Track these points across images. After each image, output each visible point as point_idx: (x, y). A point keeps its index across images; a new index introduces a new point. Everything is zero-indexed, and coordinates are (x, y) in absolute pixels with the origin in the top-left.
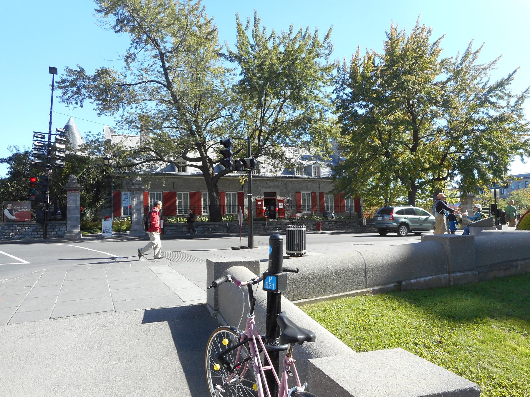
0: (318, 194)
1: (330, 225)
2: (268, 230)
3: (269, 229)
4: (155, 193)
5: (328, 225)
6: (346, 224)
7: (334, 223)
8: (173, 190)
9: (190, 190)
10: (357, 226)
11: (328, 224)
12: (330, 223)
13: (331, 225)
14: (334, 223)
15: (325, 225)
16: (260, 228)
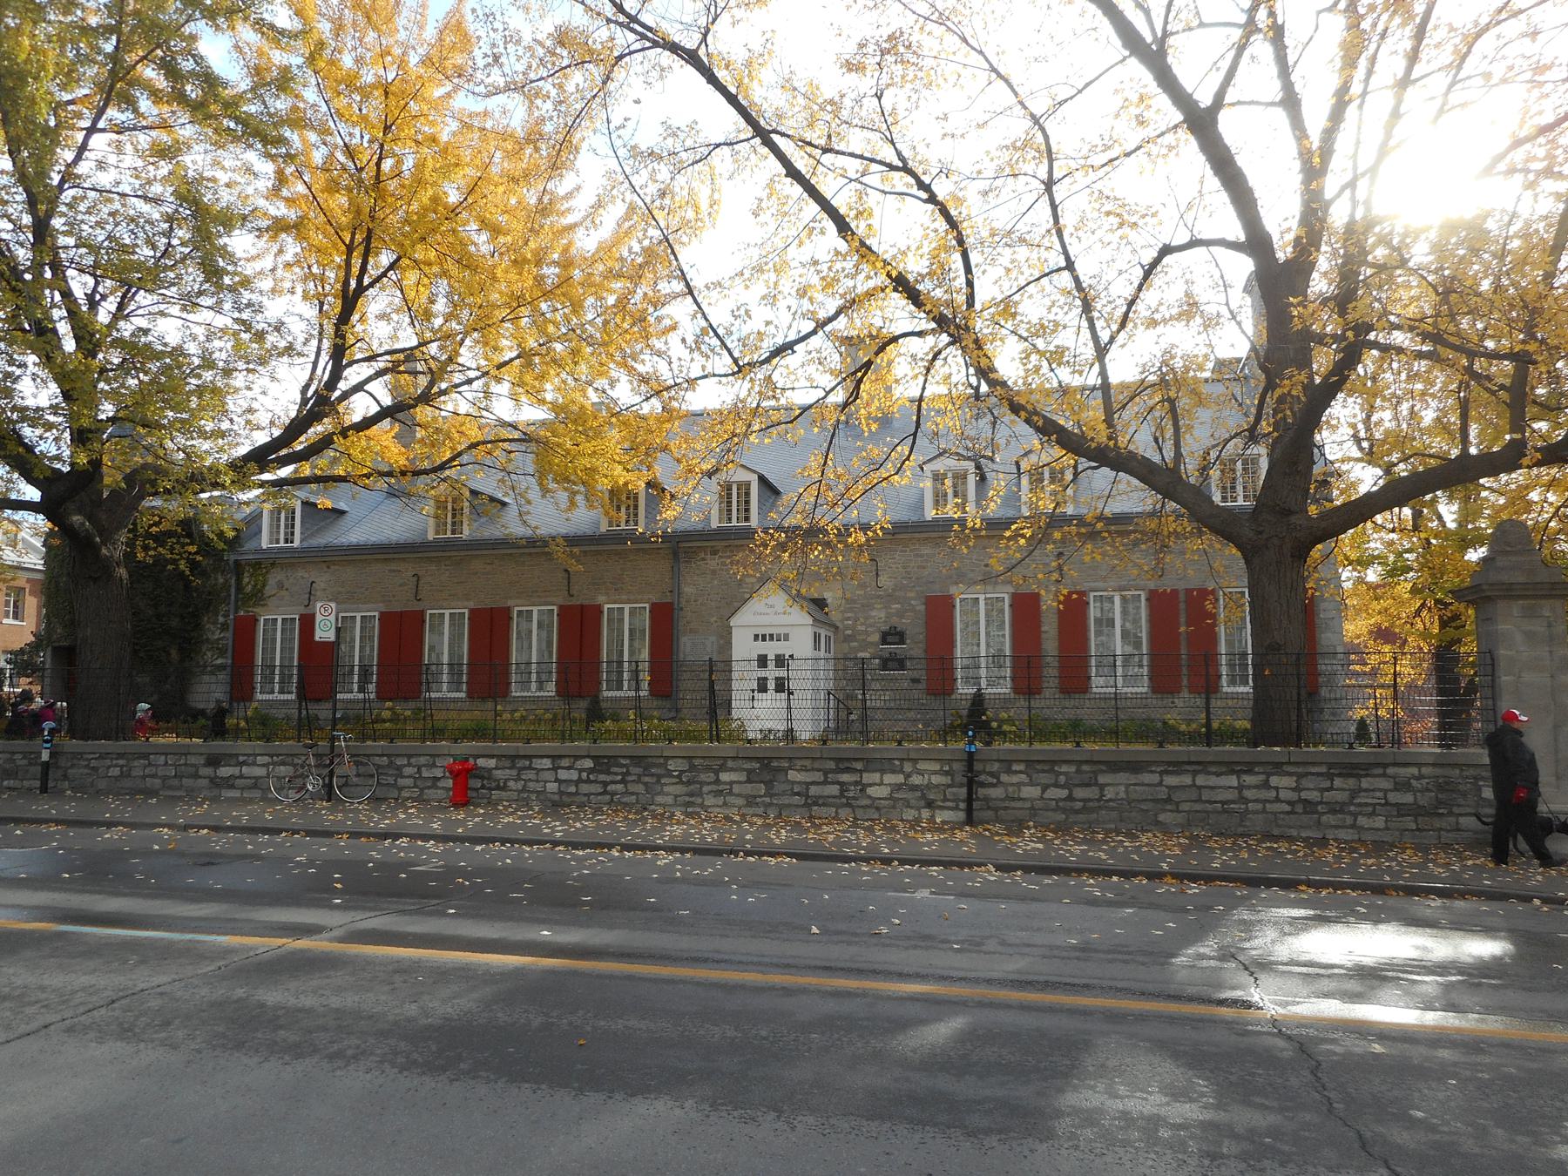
0: (1049, 603)
1: (563, 774)
2: (232, 787)
3: (238, 782)
4: (358, 616)
5: (549, 776)
6: (669, 774)
7: (589, 764)
8: (417, 607)
9: (471, 604)
10: (748, 789)
11: (555, 769)
12: (565, 762)
13: (574, 775)
14: (589, 764)
15: (531, 775)
16: (196, 776)
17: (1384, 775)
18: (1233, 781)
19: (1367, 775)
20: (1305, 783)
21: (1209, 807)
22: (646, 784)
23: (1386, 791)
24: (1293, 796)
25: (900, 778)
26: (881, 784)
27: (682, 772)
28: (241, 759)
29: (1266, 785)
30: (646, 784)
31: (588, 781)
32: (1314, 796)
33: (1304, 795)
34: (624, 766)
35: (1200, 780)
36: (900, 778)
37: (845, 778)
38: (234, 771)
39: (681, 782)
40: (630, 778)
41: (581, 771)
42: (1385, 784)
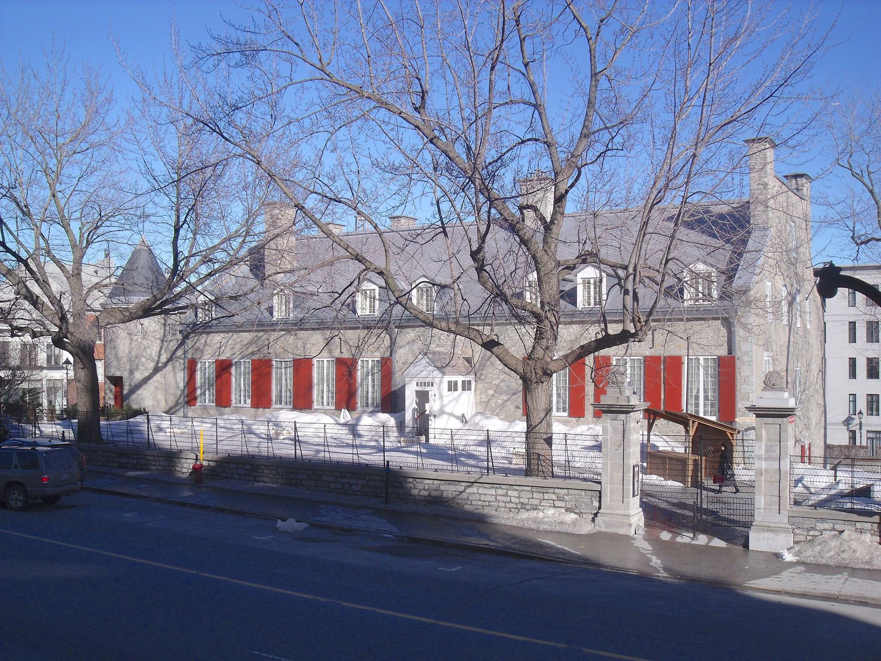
7: (249, 467)
12: (241, 466)
17: (554, 493)
18: (493, 492)
19: (547, 493)
20: (523, 494)
21: (484, 504)
22: (270, 478)
23: (554, 500)
24: (517, 500)
25: (364, 482)
26: (357, 484)
27: (283, 473)
28: (128, 455)
29: (506, 495)
30: (270, 478)
31: (249, 475)
32: (525, 501)
33: (522, 500)
34: (262, 469)
35: (481, 491)
36: (364, 482)
37: (344, 480)
38: (126, 460)
39: (283, 478)
40: (264, 475)
41: (246, 470)
42: (554, 497)
